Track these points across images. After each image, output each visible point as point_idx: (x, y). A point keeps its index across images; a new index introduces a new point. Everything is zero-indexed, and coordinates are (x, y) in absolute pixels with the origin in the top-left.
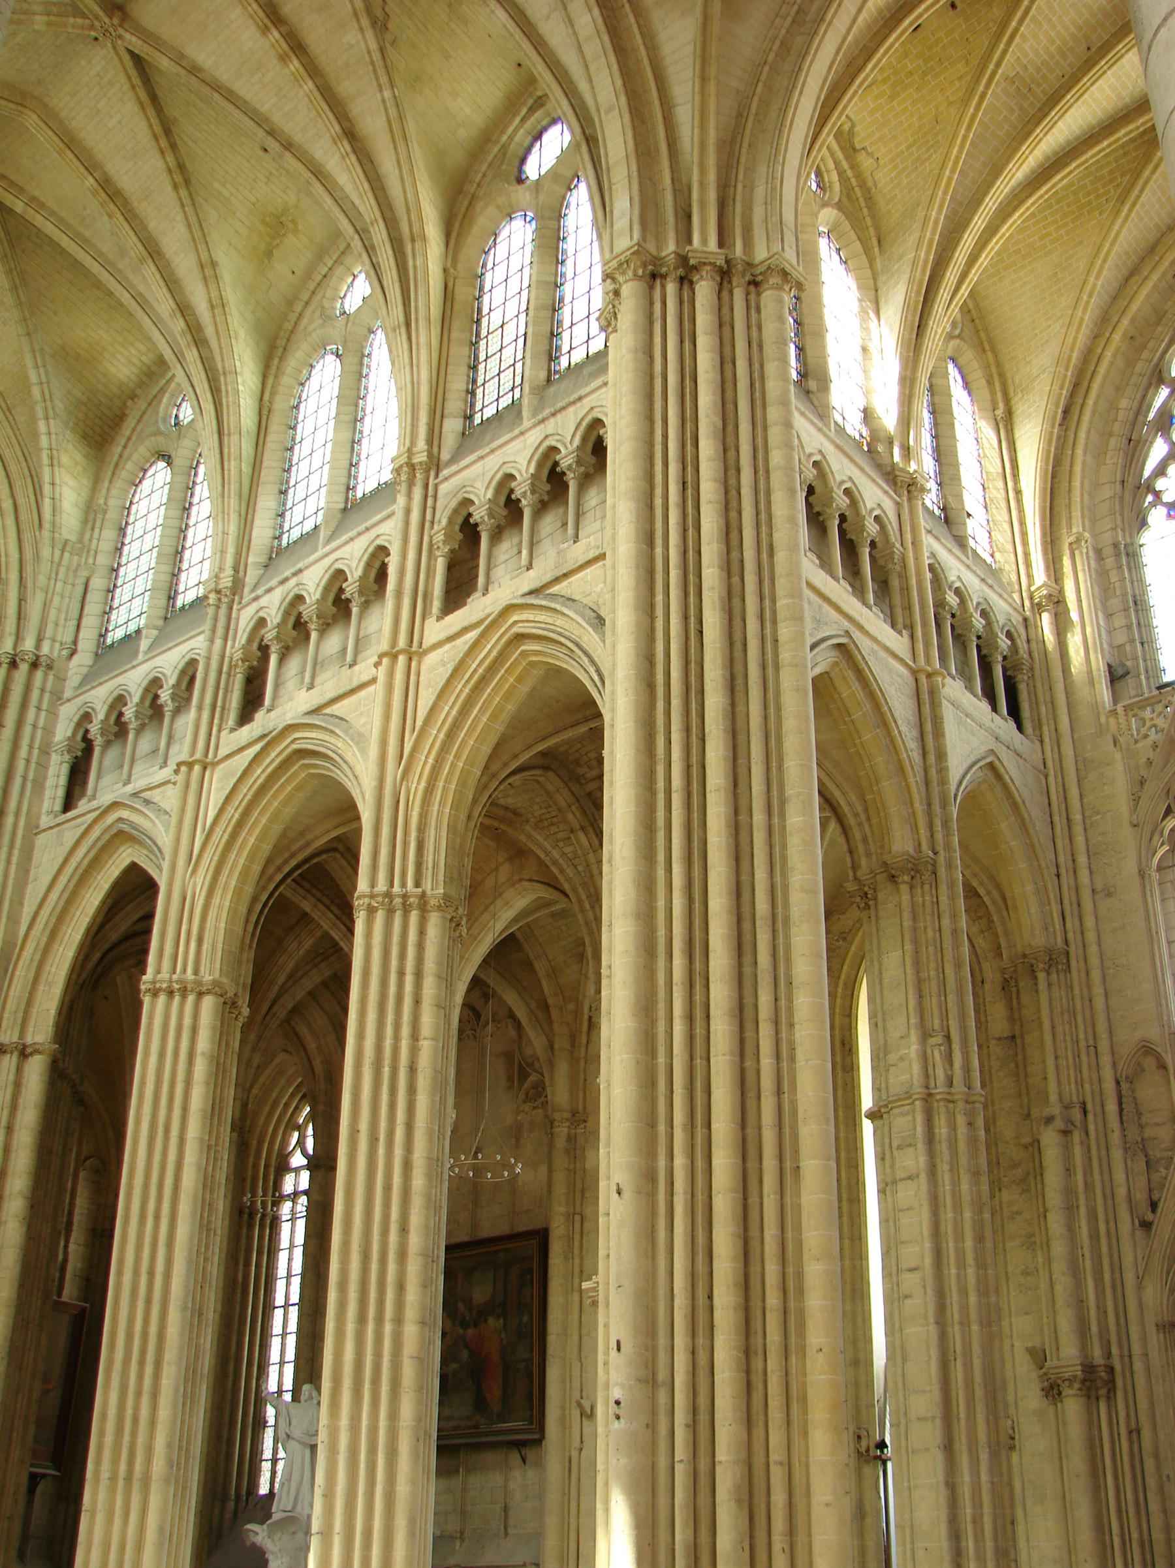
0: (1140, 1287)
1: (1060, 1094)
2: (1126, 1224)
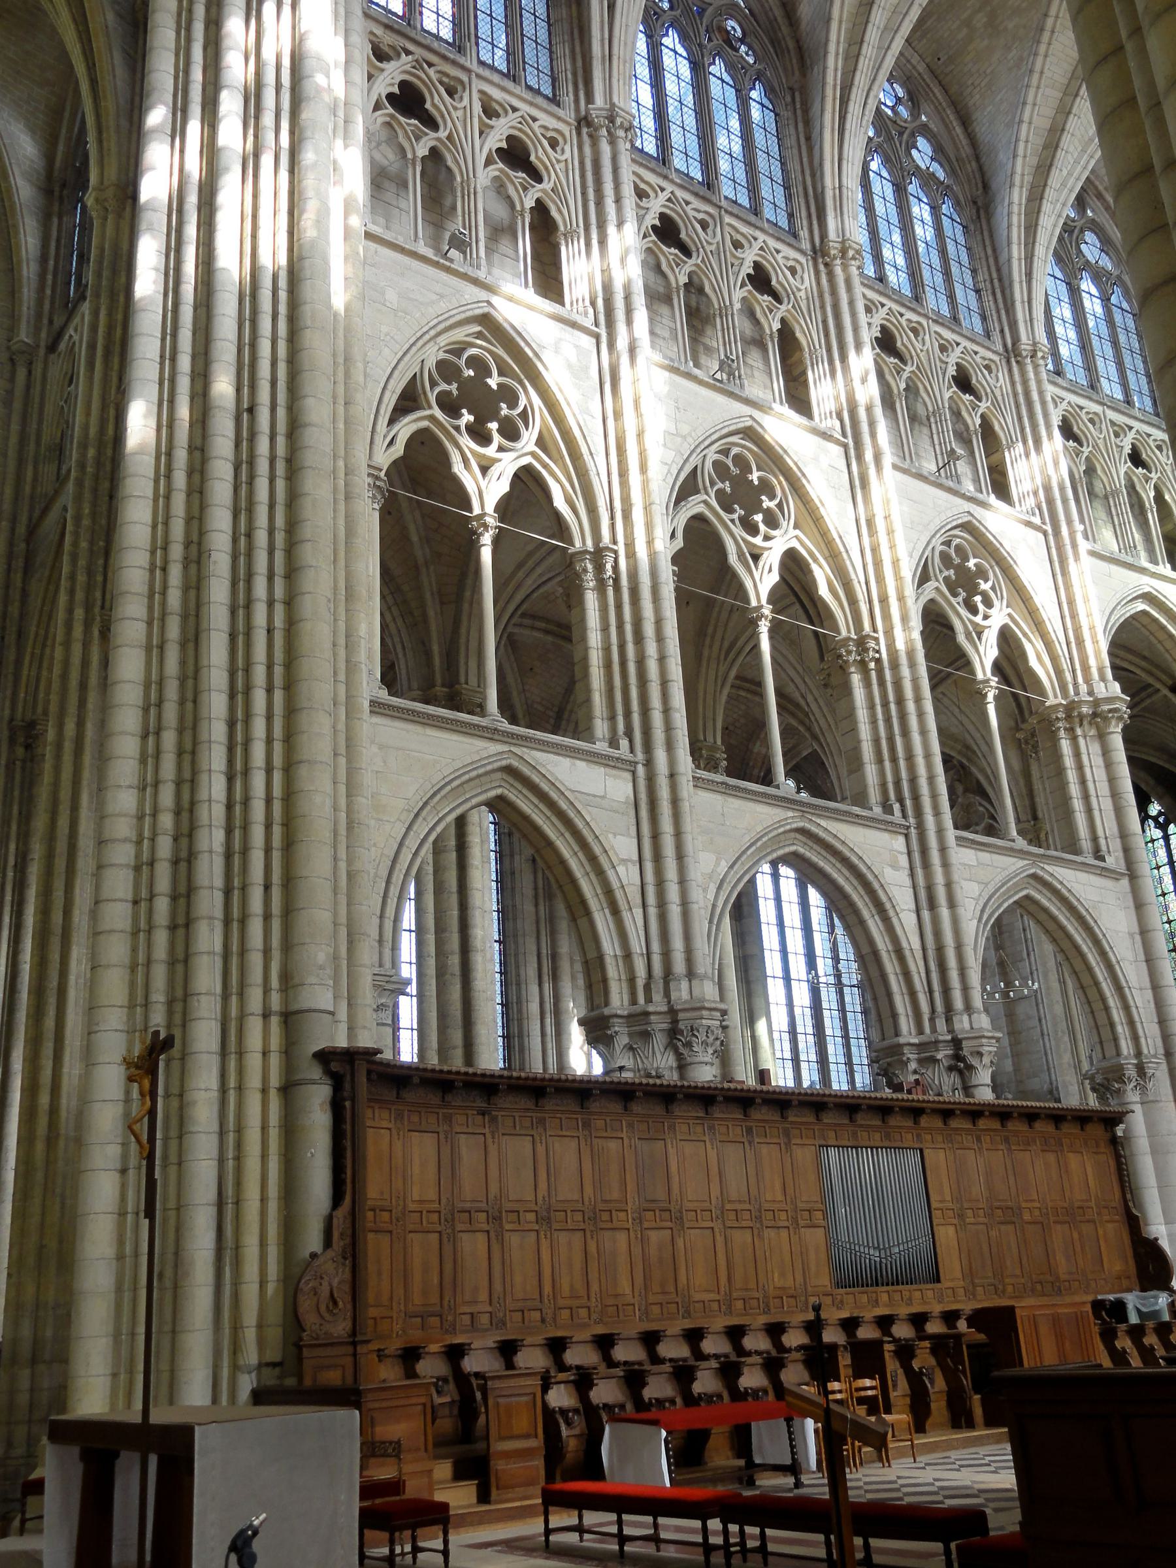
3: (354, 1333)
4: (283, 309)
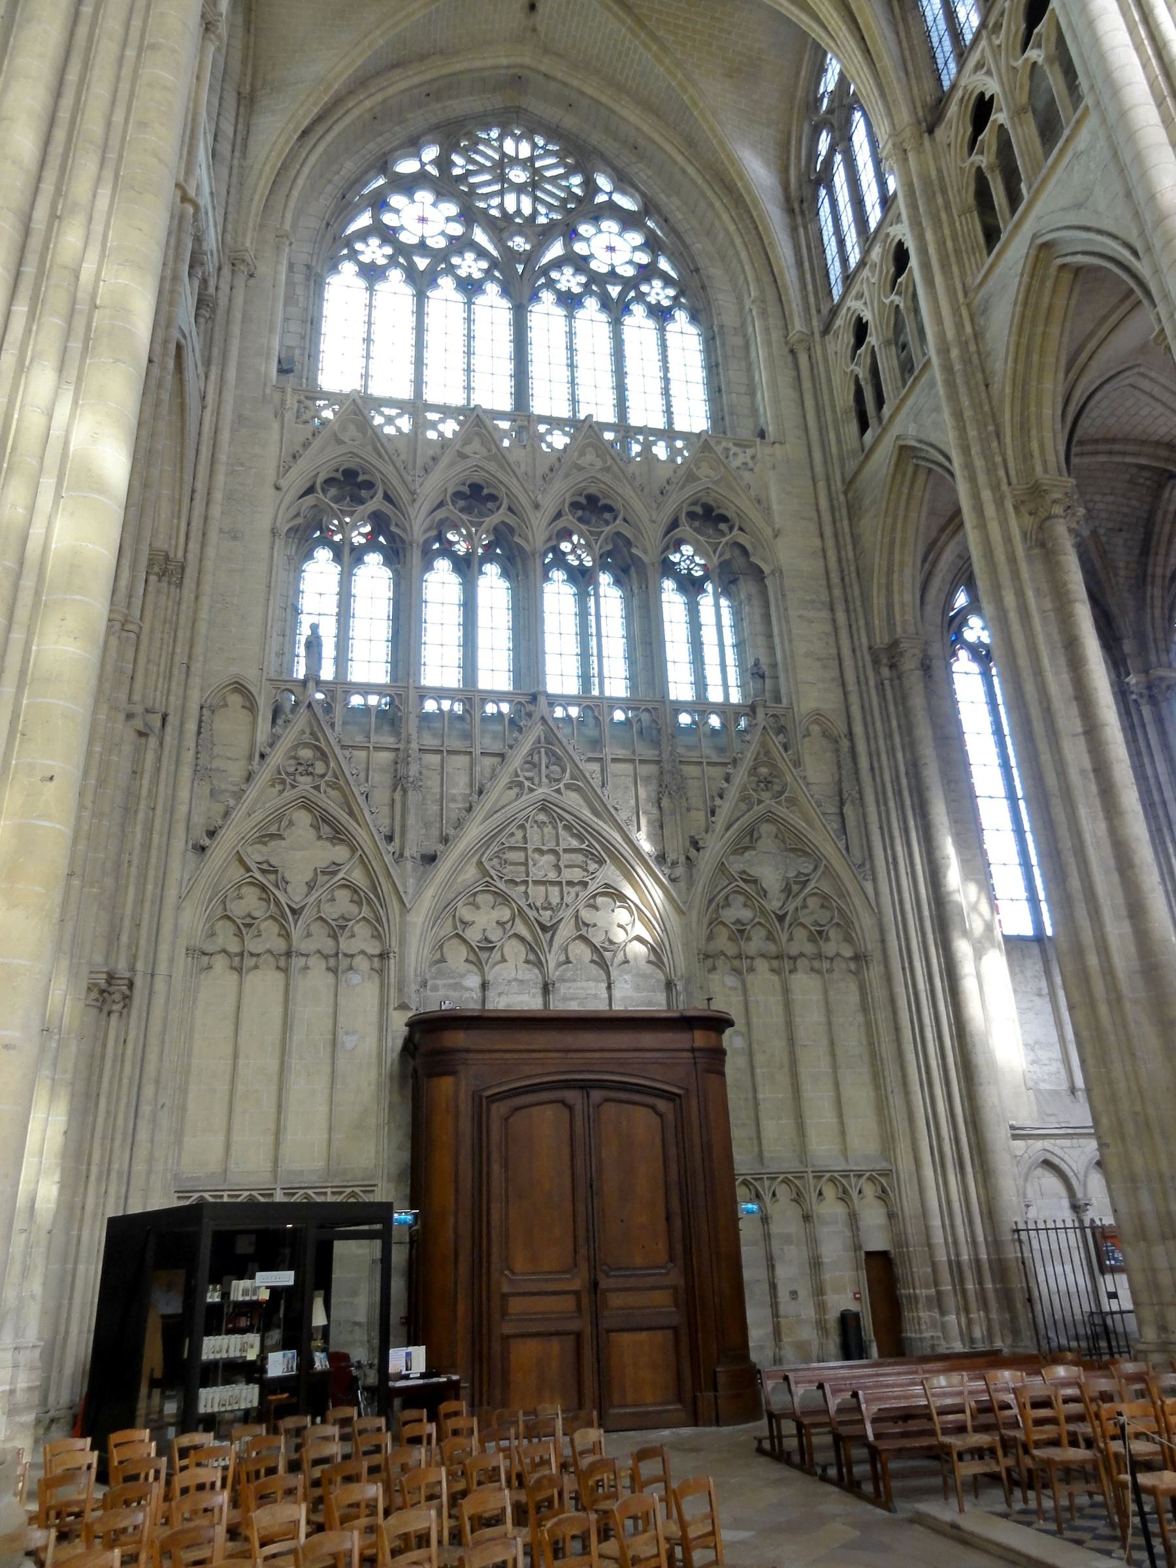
0: (178, 908)
1: (144, 697)
2: (179, 844)
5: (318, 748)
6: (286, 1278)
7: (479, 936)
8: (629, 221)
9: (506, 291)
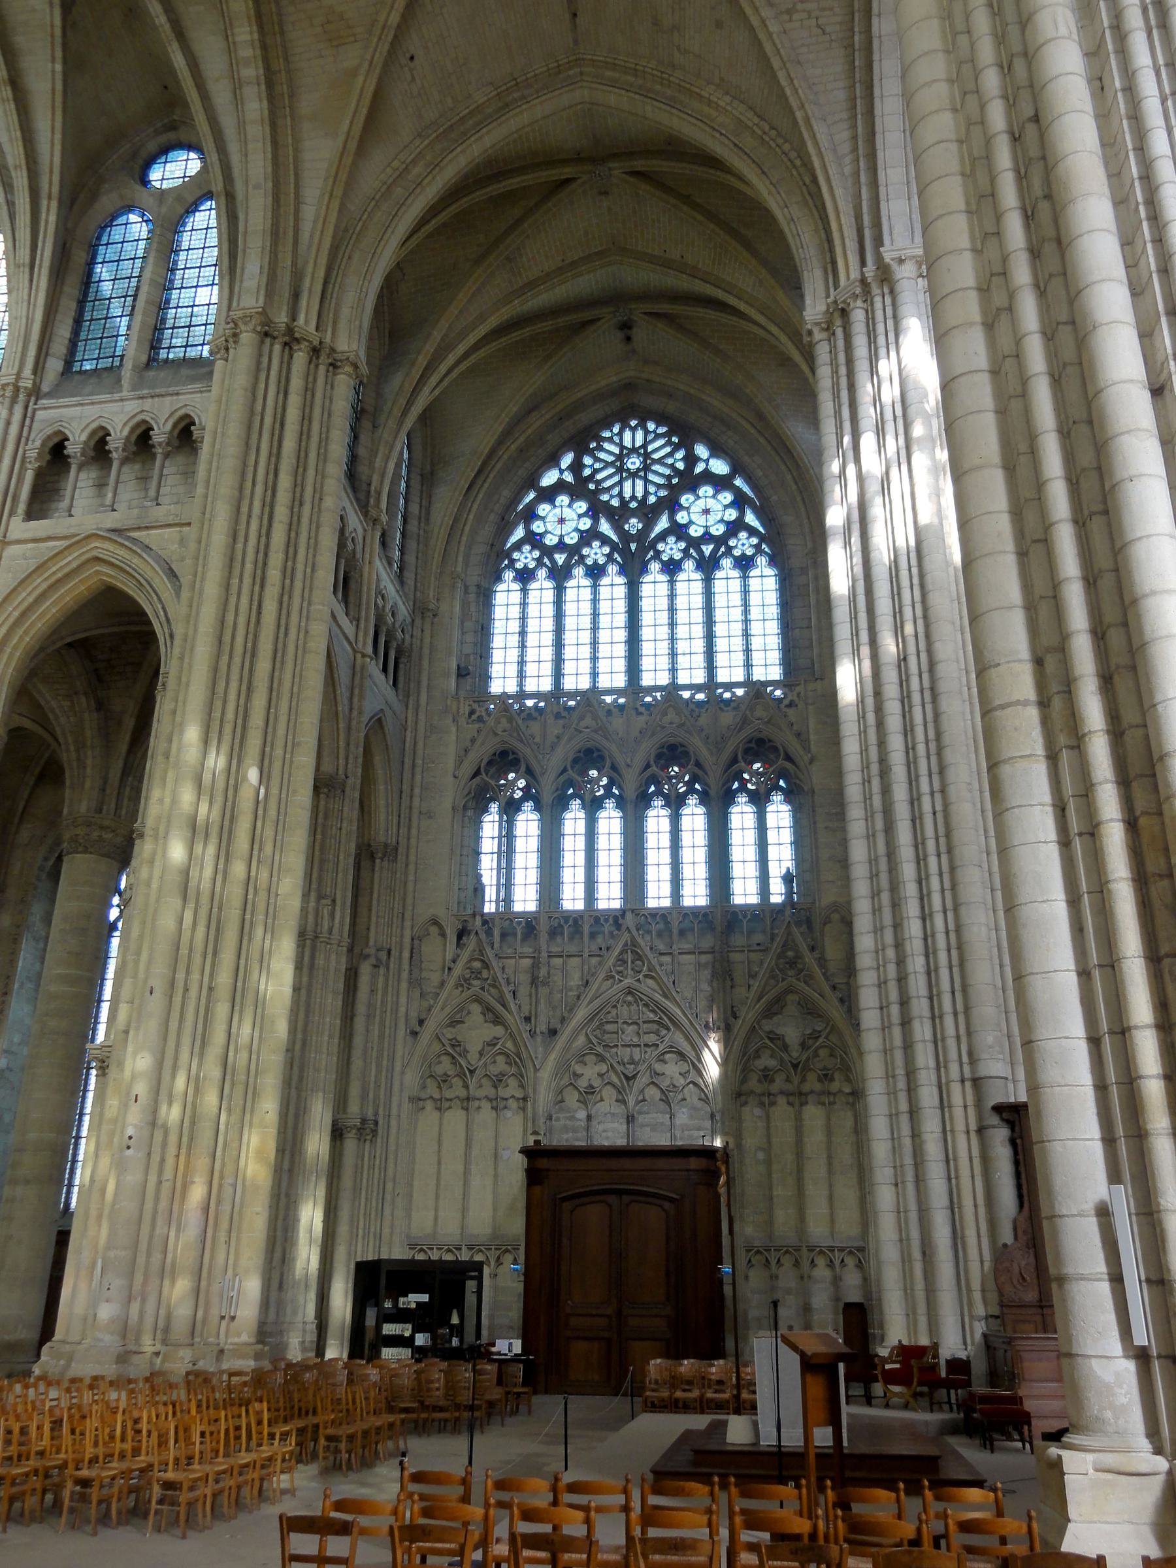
0: (403, 1073)
2: (401, 1032)
3: (1041, 1300)
4: (916, 581)
5: (483, 961)
6: (425, 1298)
7: (585, 1084)
8: (721, 483)
9: (622, 571)
